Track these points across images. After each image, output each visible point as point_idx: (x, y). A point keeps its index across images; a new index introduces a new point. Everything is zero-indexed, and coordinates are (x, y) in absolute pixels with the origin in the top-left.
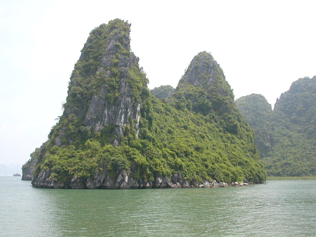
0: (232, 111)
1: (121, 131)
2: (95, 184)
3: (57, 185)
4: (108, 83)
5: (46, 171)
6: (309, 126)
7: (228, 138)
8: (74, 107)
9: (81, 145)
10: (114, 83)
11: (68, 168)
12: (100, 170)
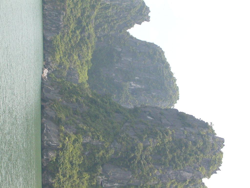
3: (44, 161)
4: (145, 185)
5: (58, 146)
8: (121, 153)
9: (83, 169)
11: (60, 171)
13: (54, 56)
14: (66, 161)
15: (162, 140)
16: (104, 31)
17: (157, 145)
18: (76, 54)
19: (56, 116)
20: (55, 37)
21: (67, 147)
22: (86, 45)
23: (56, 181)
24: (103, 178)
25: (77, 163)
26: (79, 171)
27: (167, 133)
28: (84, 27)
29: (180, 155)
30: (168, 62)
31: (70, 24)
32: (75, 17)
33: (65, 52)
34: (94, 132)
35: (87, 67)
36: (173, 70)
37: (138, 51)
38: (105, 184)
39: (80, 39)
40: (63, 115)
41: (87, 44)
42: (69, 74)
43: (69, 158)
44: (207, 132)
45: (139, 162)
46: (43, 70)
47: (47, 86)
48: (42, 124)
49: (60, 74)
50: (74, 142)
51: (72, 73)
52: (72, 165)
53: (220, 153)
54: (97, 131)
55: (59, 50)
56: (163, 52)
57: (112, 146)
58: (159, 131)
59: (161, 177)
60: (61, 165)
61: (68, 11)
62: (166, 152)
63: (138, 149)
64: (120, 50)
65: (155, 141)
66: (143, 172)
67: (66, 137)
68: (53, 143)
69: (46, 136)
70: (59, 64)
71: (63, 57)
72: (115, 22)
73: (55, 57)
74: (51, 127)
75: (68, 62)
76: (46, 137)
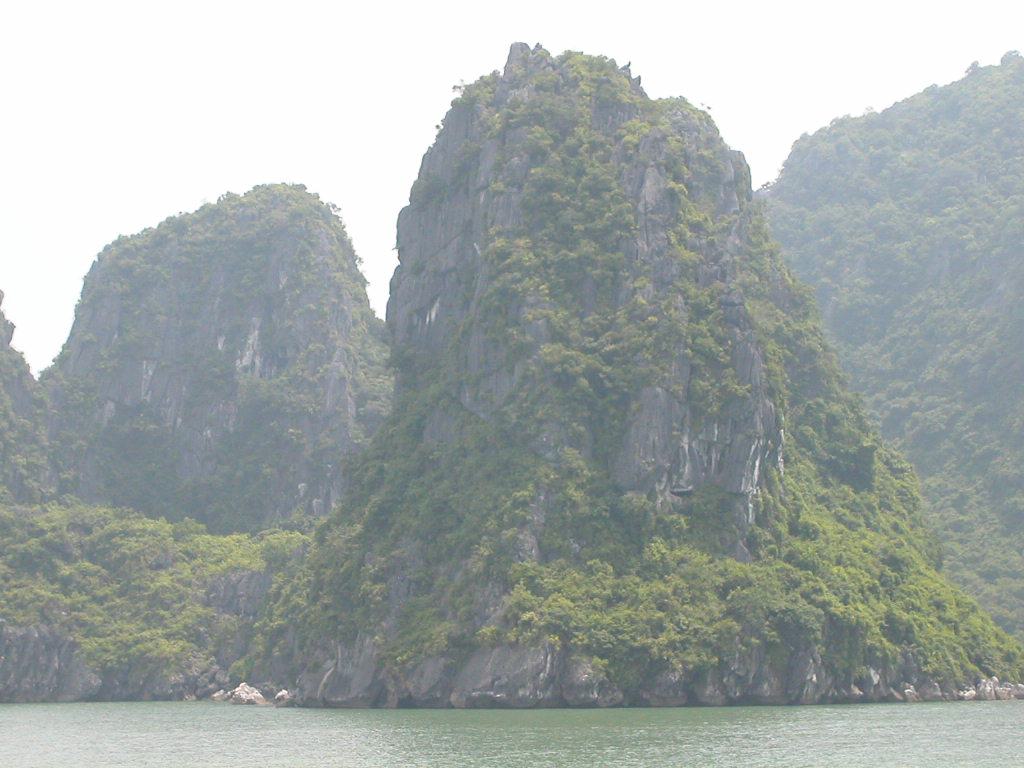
0: (836, 385)
1: (750, 511)
2: (724, 688)
3: (608, 698)
6: (914, 398)
7: (853, 507)
8: (575, 424)
10: (710, 342)
11: (641, 641)
12: (747, 645)
13: (164, 662)
14: (608, 620)
15: (528, 272)
16: (36, 466)
17: (547, 291)
18: (152, 580)
19: (443, 654)
20: (90, 655)
21: (560, 618)
22: (116, 540)
23: (677, 656)
24: (662, 488)
25: (610, 581)
26: (638, 574)
27: (503, 255)
28: (44, 544)
29: (582, 209)
30: (160, 225)
31: (38, 597)
32: (6, 579)
33: (146, 619)
34: (500, 518)
35: (198, 539)
36: (188, 204)
37: (116, 336)
38: (682, 483)
39: (93, 560)
40: (438, 629)
41: (112, 535)
42: (228, 606)
43: (595, 608)
44: (488, 105)
45: (608, 359)
46: (239, 701)
47: (321, 686)
48: (473, 704)
49: (232, 637)
50: (537, 590)
51: (223, 595)
52: (620, 599)
53: (571, 62)
54: (496, 508)
55: (137, 642)
57: (549, 455)
58: (497, 284)
59: (661, 283)
60: (620, 637)
62: (572, 260)
63: (562, 363)
64: (111, 406)
65: (531, 299)
66: (645, 346)
67: (519, 619)
68: (545, 667)
69: (516, 691)
70: (193, 642)
71: (166, 626)
73: (167, 659)
74: (483, 672)
75: (184, 607)
76: (521, 693)
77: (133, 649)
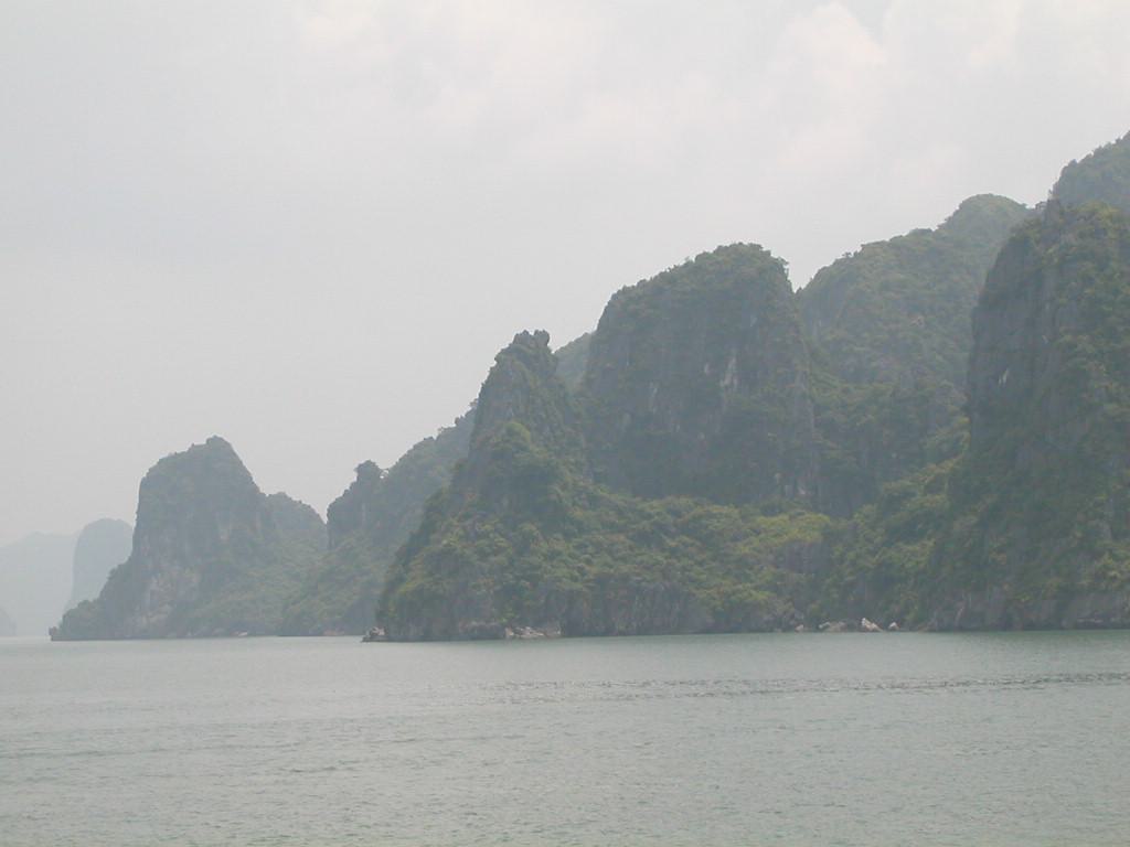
22: (704, 522)
32: (631, 548)
48: (1078, 627)
50: (1113, 556)
55: (734, 593)
56: (625, 291)
61: (625, 568)
71: (751, 582)
72: (558, 433)
75: (762, 568)
77: (733, 598)
